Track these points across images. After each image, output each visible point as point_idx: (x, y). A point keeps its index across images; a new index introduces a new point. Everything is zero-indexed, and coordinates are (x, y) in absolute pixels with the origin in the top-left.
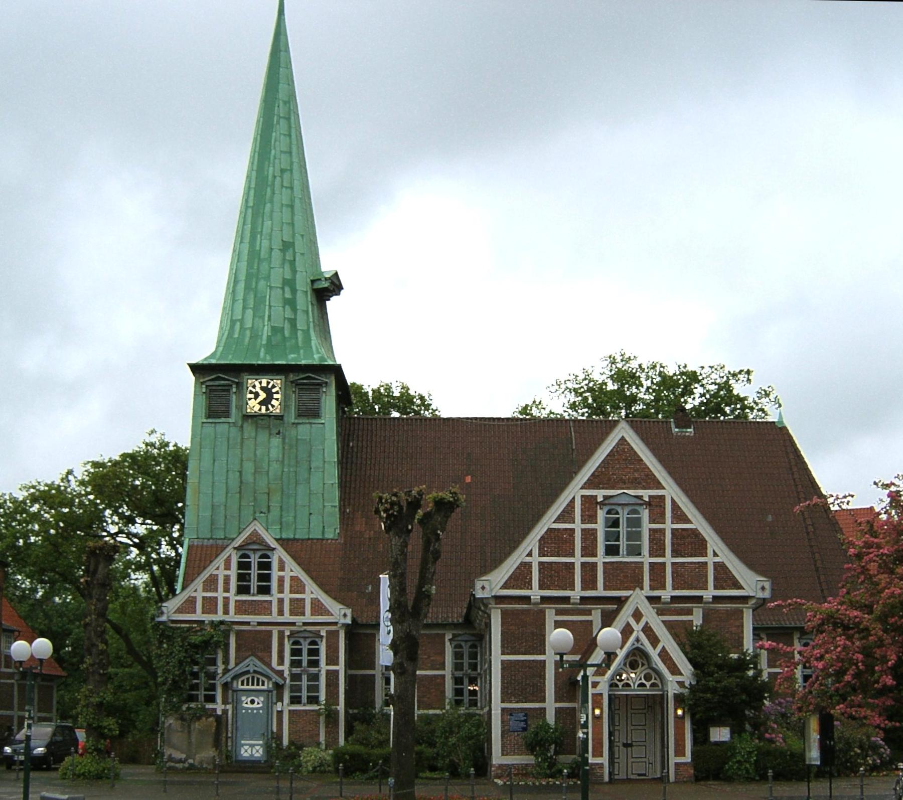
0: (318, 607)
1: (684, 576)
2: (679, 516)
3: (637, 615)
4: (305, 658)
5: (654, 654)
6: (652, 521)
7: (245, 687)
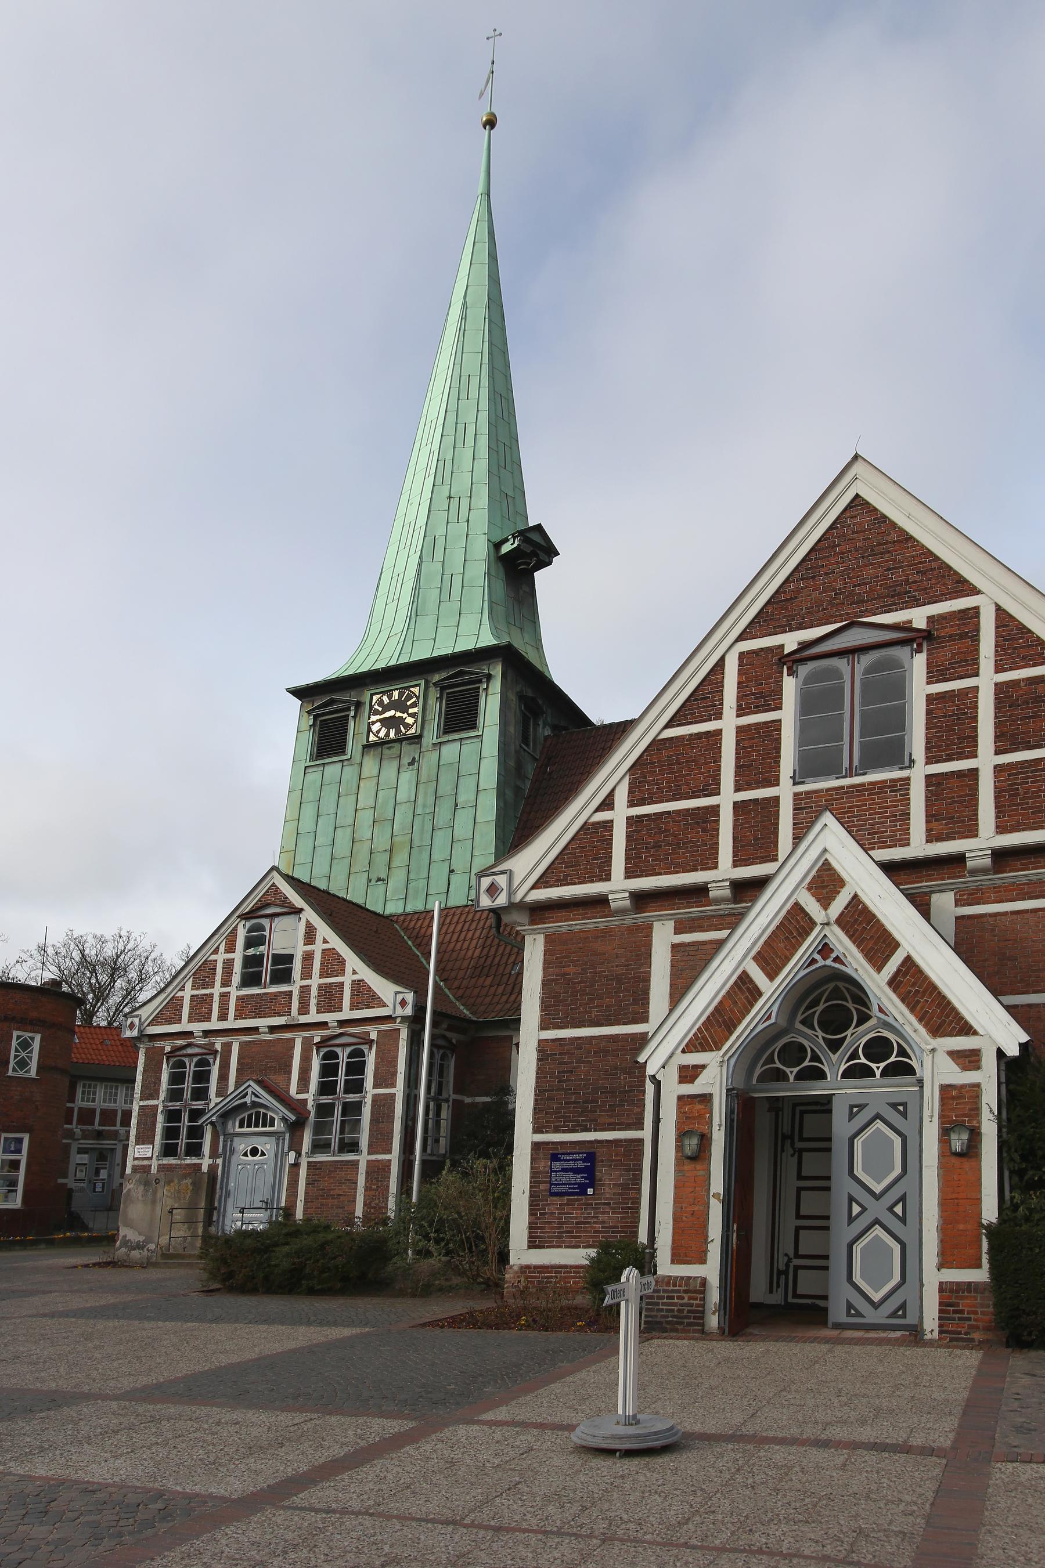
0: (363, 995)
5: (876, 983)
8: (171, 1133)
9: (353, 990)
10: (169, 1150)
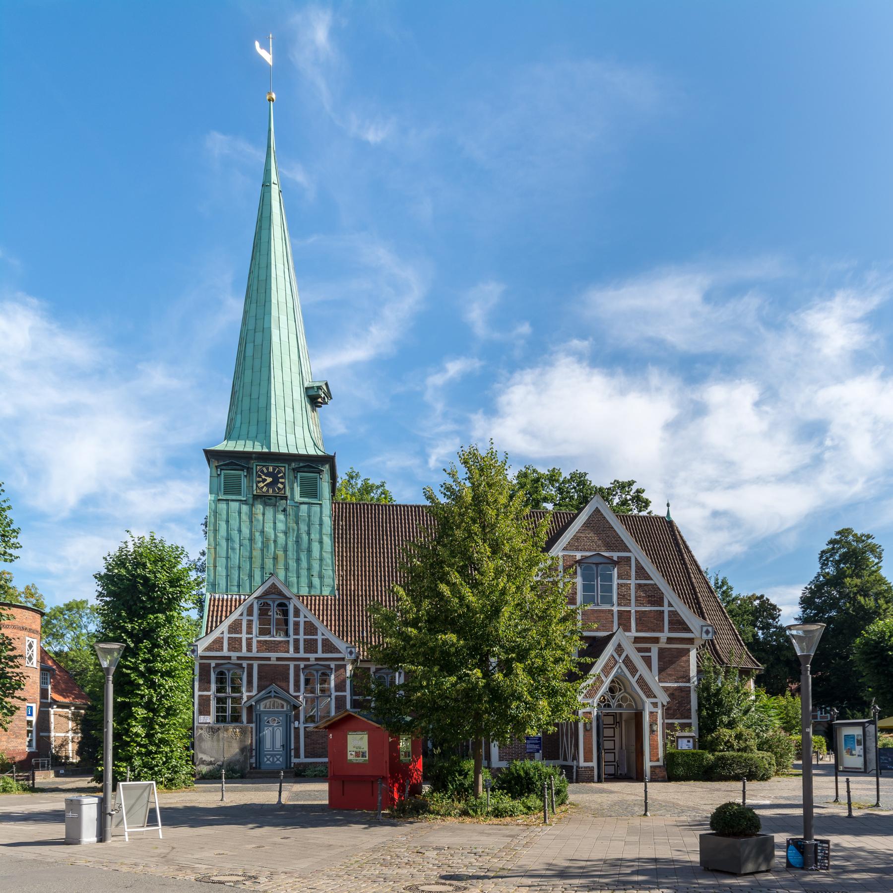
0: (328, 646)
1: (643, 621)
2: (641, 572)
3: (619, 649)
6: (620, 577)
10: (219, 719)
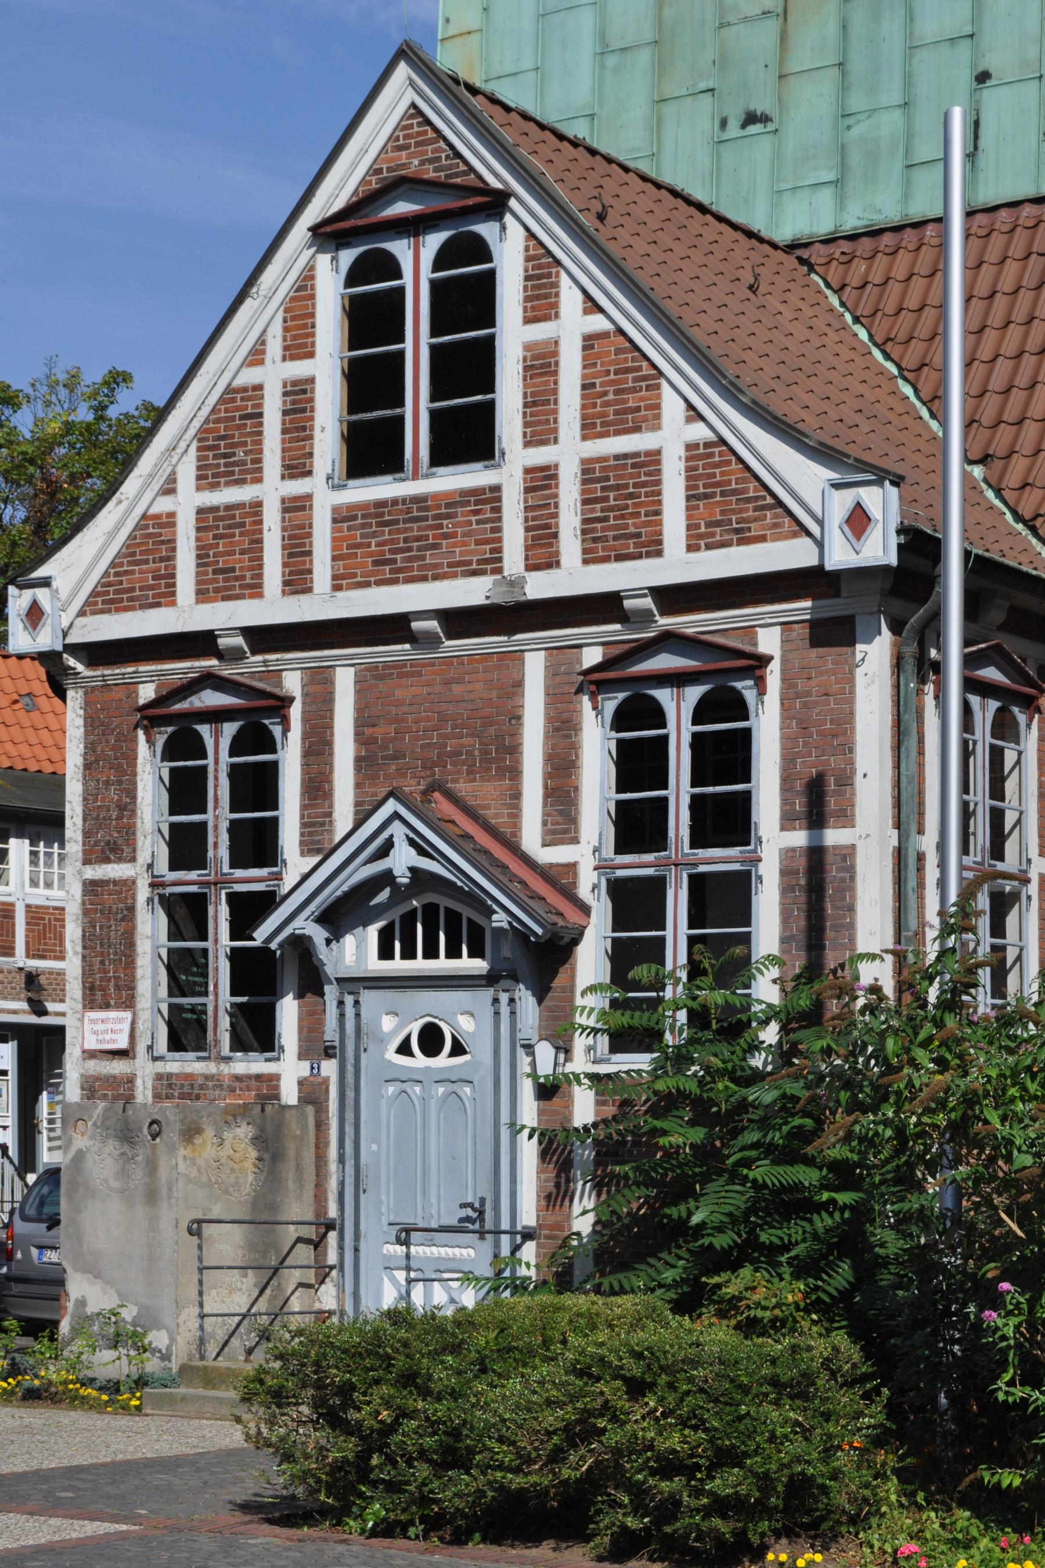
4: (680, 790)
7: (398, 966)
8: (185, 971)
9: (691, 477)
